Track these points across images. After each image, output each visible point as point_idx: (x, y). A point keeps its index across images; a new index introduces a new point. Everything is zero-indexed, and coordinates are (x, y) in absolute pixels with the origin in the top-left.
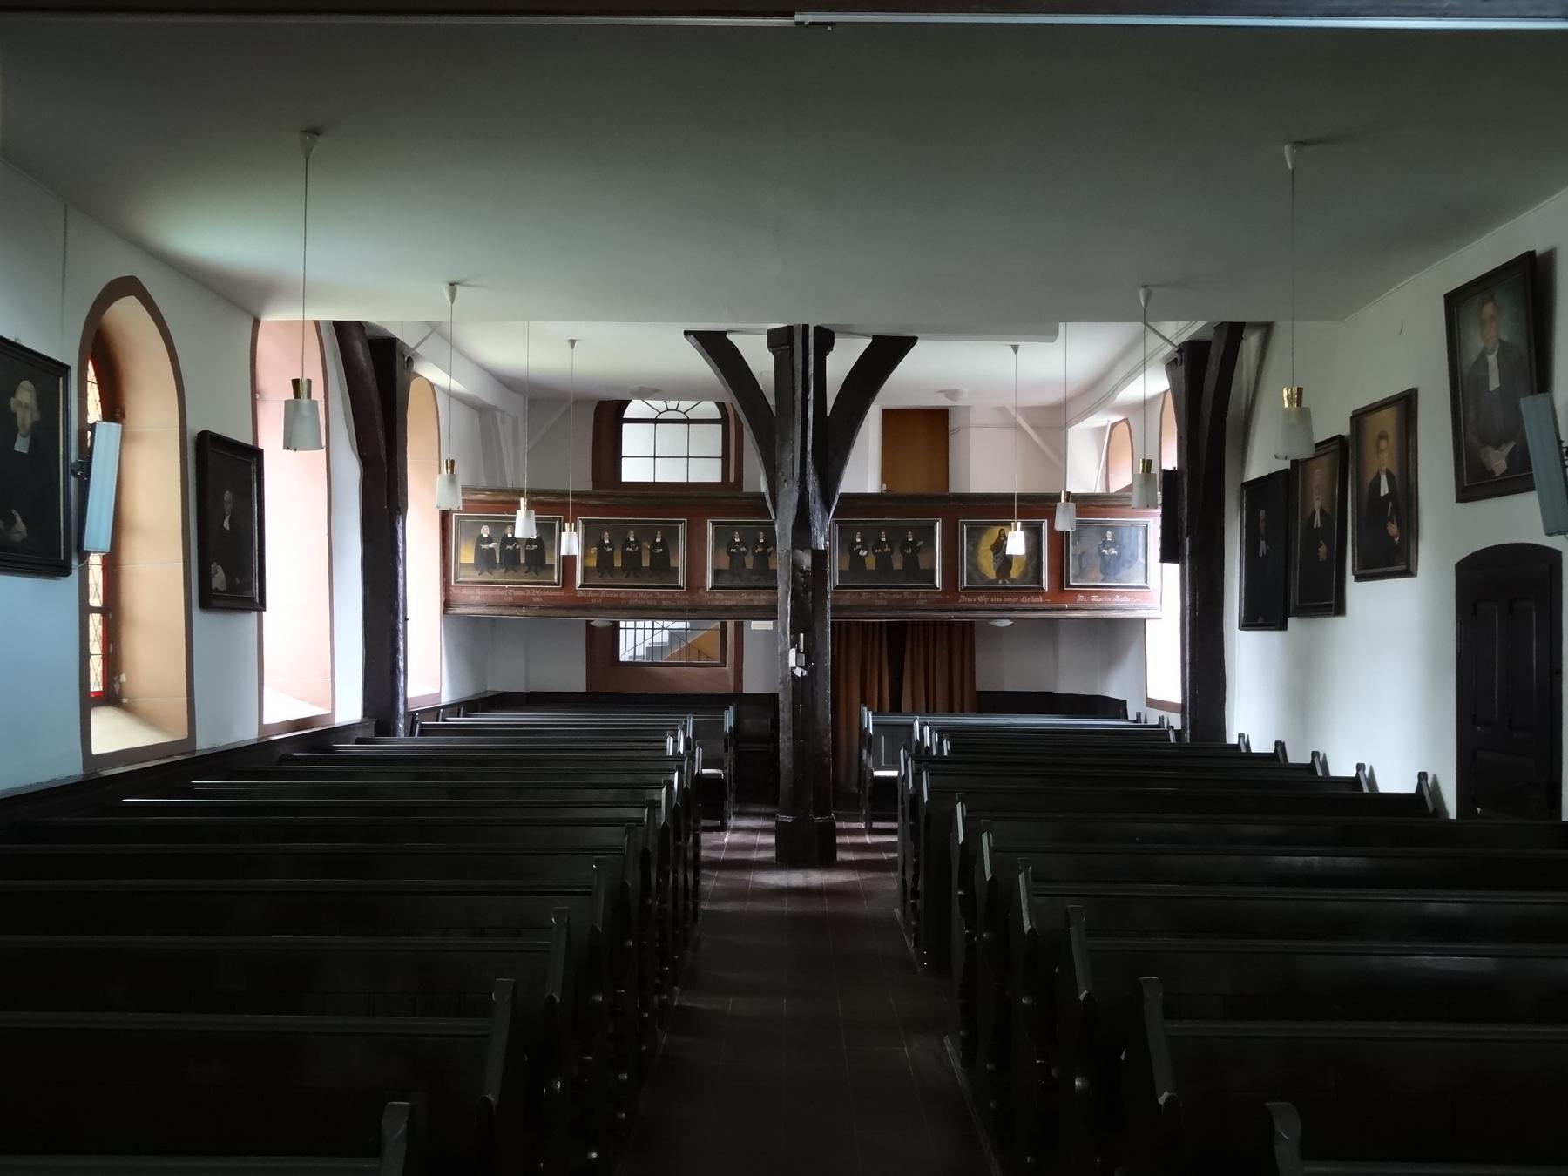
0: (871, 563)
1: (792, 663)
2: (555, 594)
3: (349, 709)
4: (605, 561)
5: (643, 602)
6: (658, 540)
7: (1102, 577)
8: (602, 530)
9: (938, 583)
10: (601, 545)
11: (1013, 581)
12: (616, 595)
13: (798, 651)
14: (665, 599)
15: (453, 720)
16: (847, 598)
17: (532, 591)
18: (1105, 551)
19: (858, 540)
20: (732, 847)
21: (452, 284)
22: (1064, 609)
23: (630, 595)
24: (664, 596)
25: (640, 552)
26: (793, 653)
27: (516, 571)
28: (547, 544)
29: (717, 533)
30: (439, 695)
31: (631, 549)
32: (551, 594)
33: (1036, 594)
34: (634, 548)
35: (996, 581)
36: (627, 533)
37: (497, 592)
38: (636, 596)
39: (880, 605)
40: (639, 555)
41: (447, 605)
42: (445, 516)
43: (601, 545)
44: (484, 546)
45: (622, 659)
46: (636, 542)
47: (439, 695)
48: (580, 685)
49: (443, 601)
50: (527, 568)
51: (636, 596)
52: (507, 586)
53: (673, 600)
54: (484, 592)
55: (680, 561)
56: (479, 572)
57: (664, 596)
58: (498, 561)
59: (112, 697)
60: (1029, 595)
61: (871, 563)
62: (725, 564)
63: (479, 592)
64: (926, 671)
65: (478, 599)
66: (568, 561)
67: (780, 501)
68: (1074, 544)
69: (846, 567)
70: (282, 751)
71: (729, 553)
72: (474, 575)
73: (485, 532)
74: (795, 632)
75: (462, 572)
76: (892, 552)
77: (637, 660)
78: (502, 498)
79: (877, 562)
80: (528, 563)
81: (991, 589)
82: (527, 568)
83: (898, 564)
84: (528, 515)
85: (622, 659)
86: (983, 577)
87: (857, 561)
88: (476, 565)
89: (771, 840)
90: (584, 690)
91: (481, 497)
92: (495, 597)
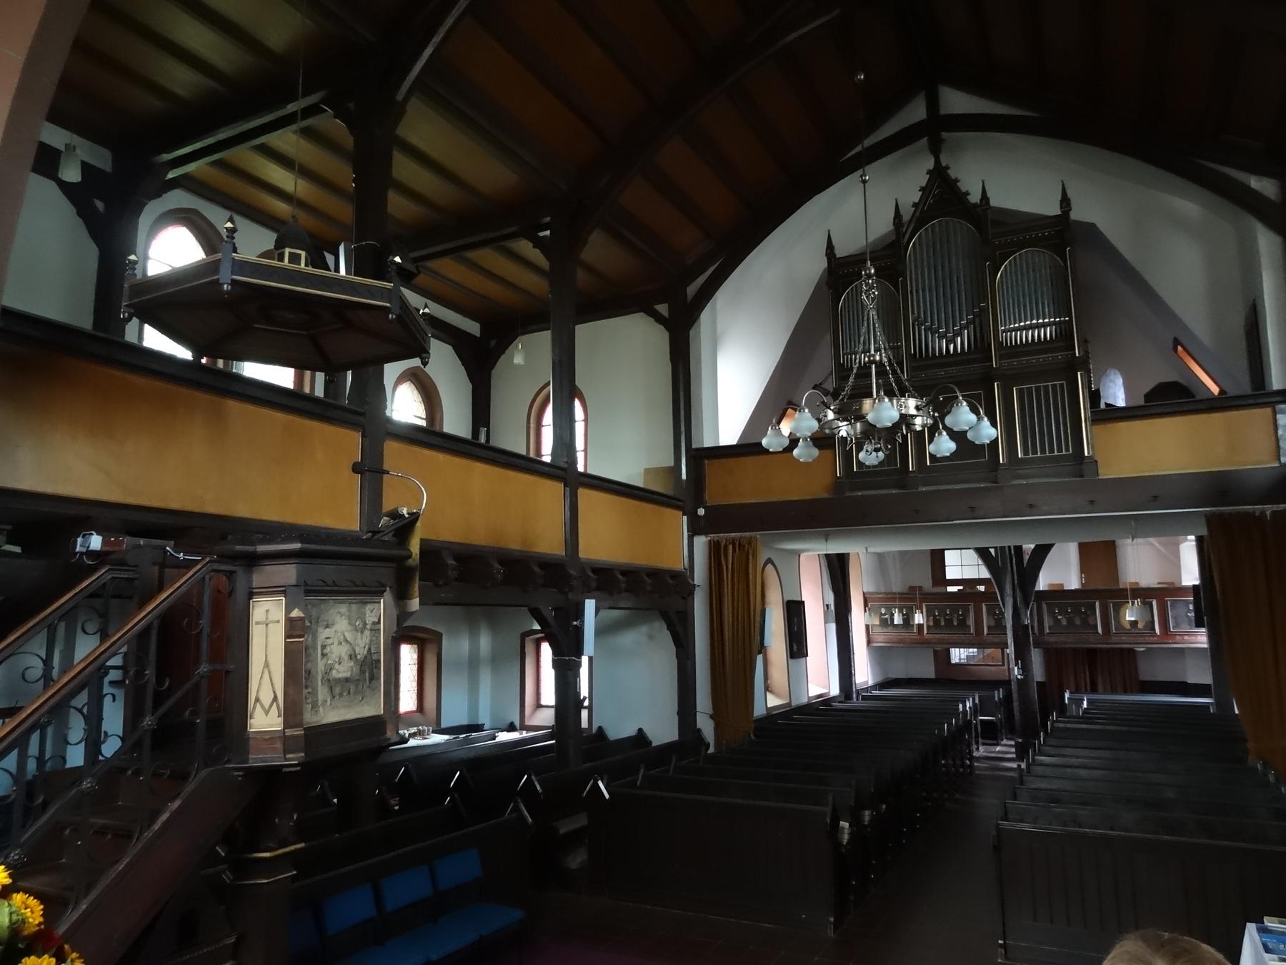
0: (1064, 622)
1: (1016, 673)
3: (835, 691)
4: (936, 622)
6: (960, 613)
7: (1188, 627)
9: (1100, 630)
10: (935, 616)
11: (1140, 630)
13: (1018, 668)
16: (1053, 639)
17: (906, 636)
18: (1189, 614)
19: (1057, 611)
20: (999, 752)
22: (1170, 643)
26: (1016, 668)
28: (911, 616)
29: (987, 609)
30: (867, 682)
32: (914, 637)
33: (1153, 636)
35: (1130, 630)
37: (890, 637)
39: (1068, 641)
40: (951, 620)
41: (869, 642)
42: (867, 627)
45: (953, 662)
47: (867, 682)
48: (932, 676)
54: (884, 637)
60: (1149, 636)
61: (1064, 622)
62: (993, 623)
63: (882, 637)
65: (881, 640)
66: (920, 626)
69: (1052, 624)
70: (816, 706)
71: (994, 619)
72: (880, 630)
73: (883, 611)
77: (962, 661)
78: (890, 596)
81: (1127, 633)
83: (1078, 622)
84: (899, 616)
85: (953, 662)
86: (1124, 628)
88: (880, 625)
89: (1013, 750)
91: (880, 596)
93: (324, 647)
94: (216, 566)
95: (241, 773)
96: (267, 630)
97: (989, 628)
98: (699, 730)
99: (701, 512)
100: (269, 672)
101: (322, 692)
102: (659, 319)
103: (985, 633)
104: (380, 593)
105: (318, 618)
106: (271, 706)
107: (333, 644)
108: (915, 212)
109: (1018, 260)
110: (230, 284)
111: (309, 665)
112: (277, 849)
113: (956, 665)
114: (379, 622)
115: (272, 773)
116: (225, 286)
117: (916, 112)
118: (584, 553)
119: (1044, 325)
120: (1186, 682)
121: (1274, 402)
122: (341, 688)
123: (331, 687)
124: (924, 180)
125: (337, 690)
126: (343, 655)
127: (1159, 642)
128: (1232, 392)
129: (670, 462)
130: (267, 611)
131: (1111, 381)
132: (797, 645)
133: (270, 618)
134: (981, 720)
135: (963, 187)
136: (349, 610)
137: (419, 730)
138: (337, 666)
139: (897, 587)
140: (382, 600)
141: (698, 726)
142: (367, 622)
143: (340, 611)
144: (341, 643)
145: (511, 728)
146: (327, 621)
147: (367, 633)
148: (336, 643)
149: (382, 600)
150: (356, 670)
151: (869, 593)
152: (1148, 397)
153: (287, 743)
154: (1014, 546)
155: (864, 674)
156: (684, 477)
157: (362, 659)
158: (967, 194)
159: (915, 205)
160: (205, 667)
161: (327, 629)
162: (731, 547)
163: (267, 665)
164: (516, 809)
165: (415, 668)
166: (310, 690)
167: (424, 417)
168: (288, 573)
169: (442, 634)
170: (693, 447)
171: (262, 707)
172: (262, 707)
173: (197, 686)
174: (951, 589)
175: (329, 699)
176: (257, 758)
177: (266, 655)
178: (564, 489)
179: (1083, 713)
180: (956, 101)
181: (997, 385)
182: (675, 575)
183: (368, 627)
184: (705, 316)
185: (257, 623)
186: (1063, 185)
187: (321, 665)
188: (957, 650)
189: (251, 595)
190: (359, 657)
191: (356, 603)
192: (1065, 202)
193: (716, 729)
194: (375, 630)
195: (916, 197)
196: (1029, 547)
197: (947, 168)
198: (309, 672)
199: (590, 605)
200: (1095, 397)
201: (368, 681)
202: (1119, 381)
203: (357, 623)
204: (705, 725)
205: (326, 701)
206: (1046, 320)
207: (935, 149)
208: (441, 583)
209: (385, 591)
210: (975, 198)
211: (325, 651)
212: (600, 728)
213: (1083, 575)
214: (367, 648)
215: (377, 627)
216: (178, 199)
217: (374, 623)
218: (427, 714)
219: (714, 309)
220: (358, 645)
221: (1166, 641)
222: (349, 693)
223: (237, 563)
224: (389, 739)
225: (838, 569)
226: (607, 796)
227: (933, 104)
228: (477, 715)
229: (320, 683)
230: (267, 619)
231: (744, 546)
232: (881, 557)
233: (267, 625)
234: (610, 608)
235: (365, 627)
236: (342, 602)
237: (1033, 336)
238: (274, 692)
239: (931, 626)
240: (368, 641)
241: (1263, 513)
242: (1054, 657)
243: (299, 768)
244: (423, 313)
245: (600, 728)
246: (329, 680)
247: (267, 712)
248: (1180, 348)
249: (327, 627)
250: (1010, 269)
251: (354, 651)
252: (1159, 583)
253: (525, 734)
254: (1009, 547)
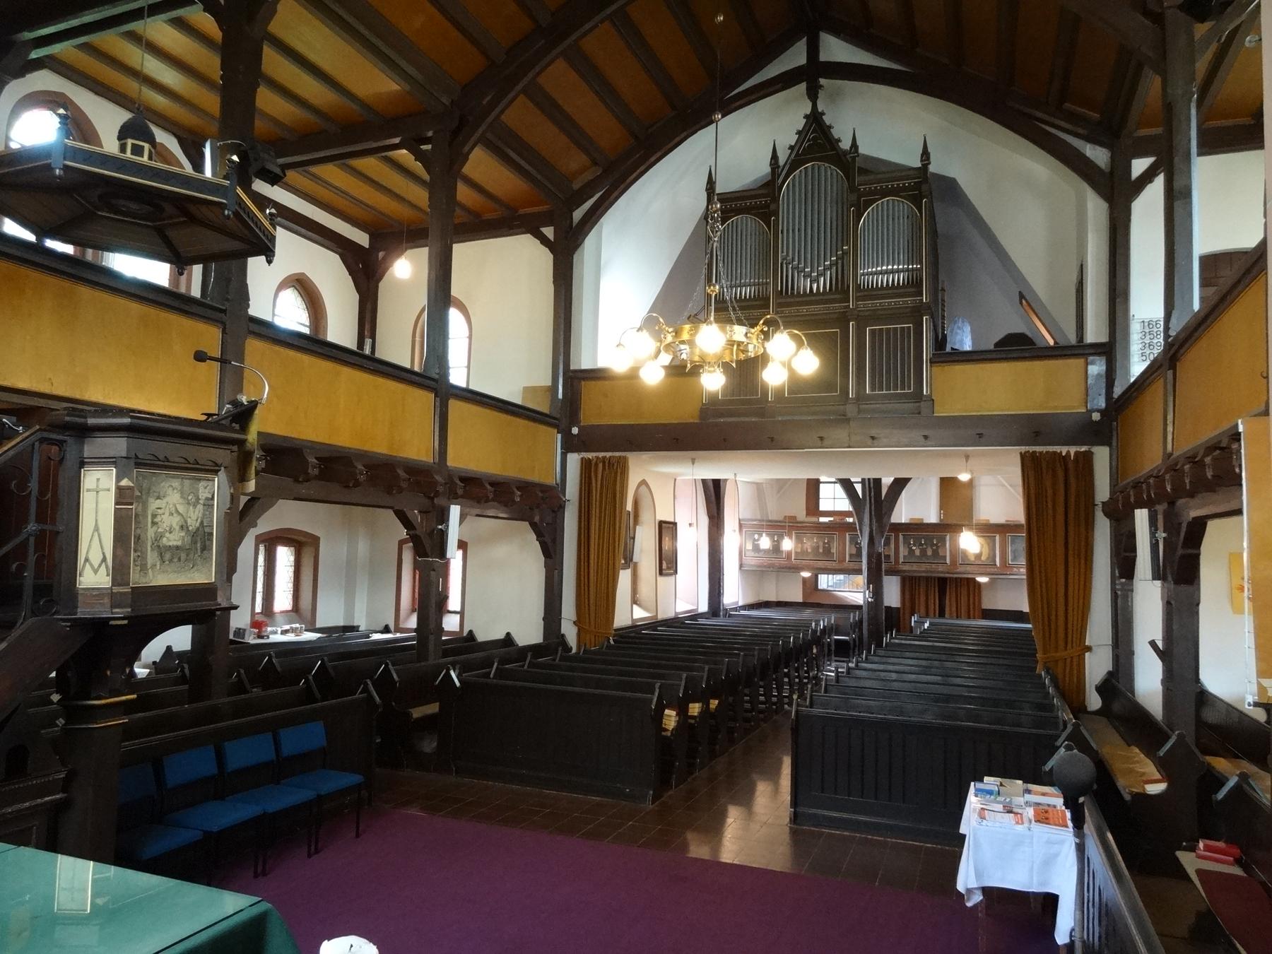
0: (918, 552)
2: (783, 562)
3: (704, 608)
13: (870, 591)
15: (743, 612)
16: (906, 567)
21: (735, 474)
22: (1007, 574)
26: (867, 592)
35: (974, 561)
37: (761, 561)
40: (818, 547)
41: (741, 566)
48: (800, 599)
55: (834, 550)
59: (635, 601)
61: (918, 552)
64: (957, 599)
67: (863, 531)
68: (1011, 546)
69: (906, 554)
72: (752, 554)
74: (869, 583)
79: (921, 552)
83: (929, 552)
86: (969, 560)
87: (911, 552)
90: (801, 601)
91: (755, 523)
93: (154, 516)
94: (46, 435)
95: (69, 624)
96: (97, 497)
97: (851, 555)
98: (563, 636)
99: (575, 430)
100: (99, 535)
101: (152, 557)
102: (544, 240)
103: (847, 560)
104: (216, 472)
105: (149, 489)
106: (100, 566)
107: (164, 514)
108: (791, 153)
109: (880, 208)
110: (62, 169)
111: (139, 531)
112: (108, 698)
113: (823, 590)
114: (213, 498)
115: (99, 625)
116: (58, 171)
117: (796, 56)
118: (451, 462)
119: (898, 271)
120: (1022, 611)
121: (1087, 354)
122: (170, 555)
123: (161, 554)
124: (800, 123)
125: (168, 556)
126: (174, 525)
127: (1001, 573)
128: (1062, 343)
129: (549, 383)
130: (98, 480)
131: (959, 328)
132: (667, 564)
133: (100, 487)
134: (836, 640)
135: (836, 133)
136: (182, 485)
137: (291, 628)
138: (167, 535)
139: (774, 516)
140: (216, 479)
141: (563, 632)
142: (200, 497)
143: (173, 485)
144: (172, 514)
145: (386, 630)
146: (159, 493)
147: (200, 507)
148: (167, 514)
149: (216, 479)
150: (188, 539)
151: (743, 520)
152: (997, 345)
153: (115, 600)
154: (873, 479)
155: (734, 594)
156: (560, 396)
157: (194, 531)
158: (839, 140)
159: (792, 148)
160: (34, 526)
161: (159, 500)
162: (601, 465)
163: (97, 529)
164: (366, 690)
165: (292, 569)
166: (139, 554)
167: (308, 324)
168: (118, 445)
169: (319, 538)
170: (571, 368)
171: (92, 566)
172: (92, 566)
173: (24, 544)
174: (822, 519)
175: (158, 563)
176: (83, 612)
177: (96, 520)
178: (435, 399)
179: (921, 633)
180: (836, 50)
181: (853, 324)
182: (545, 488)
183: (201, 502)
184: (589, 242)
185: (88, 490)
186: (925, 138)
187: (151, 533)
188: (826, 576)
189: (82, 464)
190: (190, 528)
191: (189, 479)
192: (925, 155)
193: (579, 635)
194: (209, 505)
195: (793, 139)
196: (887, 481)
197: (823, 114)
198: (138, 538)
199: (455, 511)
200: (940, 342)
201: (199, 551)
202: (968, 329)
203: (190, 498)
204: (569, 631)
205: (156, 565)
206: (901, 267)
207: (813, 94)
208: (300, 480)
209: (220, 470)
210: (845, 145)
211: (155, 520)
212: (471, 632)
213: (942, 512)
214: (199, 521)
215: (210, 502)
216: (44, 80)
217: (207, 499)
218: (300, 612)
219: (600, 234)
220: (190, 517)
221: (1005, 573)
222: (179, 560)
223: (67, 433)
224: (220, 604)
225: (714, 493)
226: (458, 684)
227: (813, 50)
228: (353, 618)
229: (149, 548)
230: (97, 486)
231: (613, 464)
232: (758, 487)
233: (97, 492)
234: (478, 515)
235: (198, 502)
236: (174, 477)
237: (893, 281)
238: (103, 554)
239: (798, 553)
240: (200, 515)
241: (1068, 452)
242: (910, 584)
243: (125, 622)
244: (270, 213)
245: (471, 632)
246: (159, 546)
247: (96, 571)
248: (1024, 301)
249: (158, 498)
250: (873, 215)
251: (187, 523)
252: (1007, 521)
253: (398, 635)
254: (869, 479)
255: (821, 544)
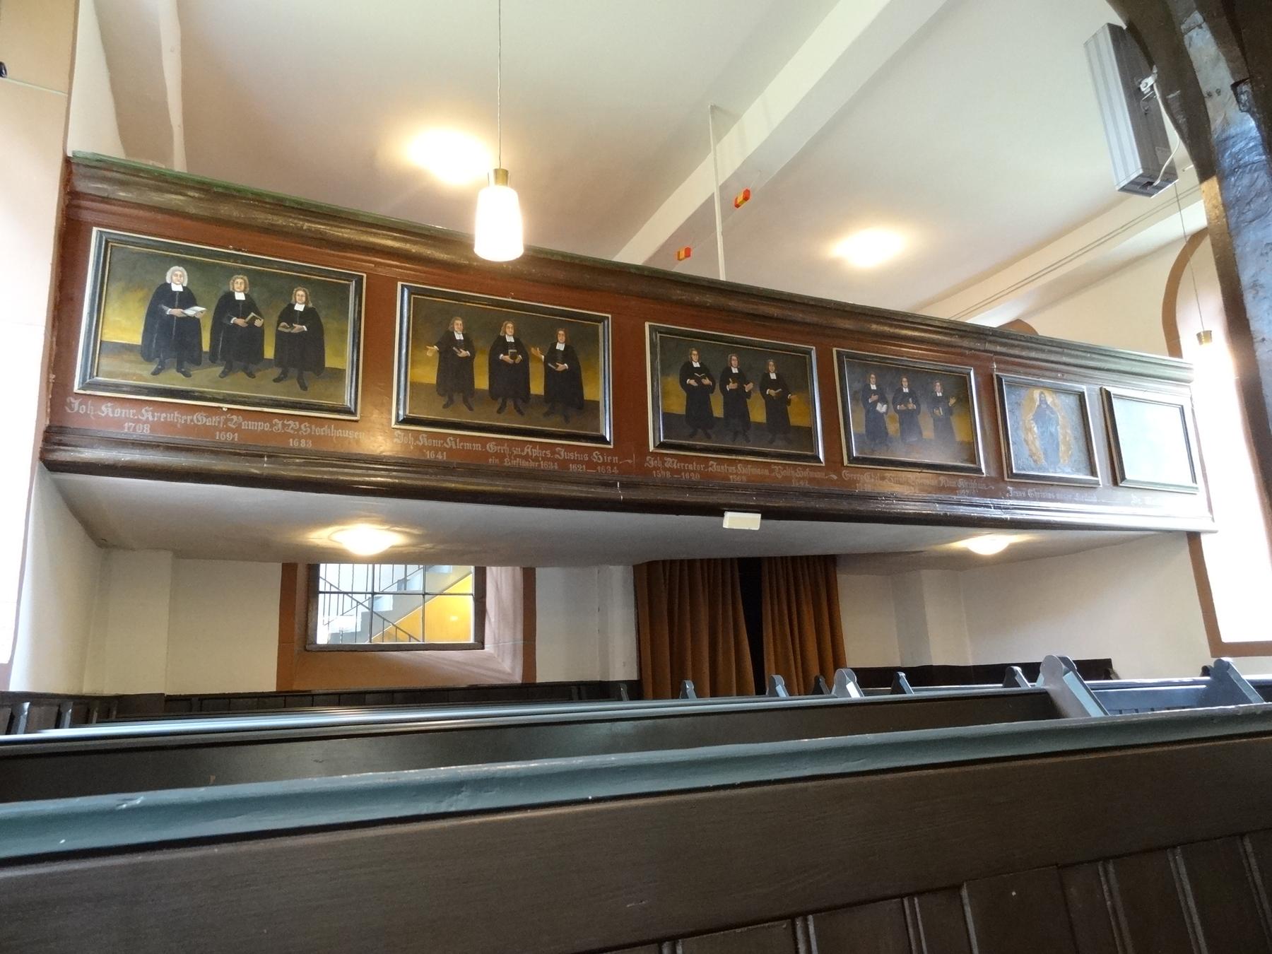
5: (532, 464)
8: (449, 315)
10: (447, 344)
12: (477, 447)
14: (574, 462)
19: (874, 387)
23: (505, 448)
24: (572, 456)
25: (525, 363)
27: (251, 375)
31: (507, 358)
34: (513, 356)
36: (499, 326)
37: (200, 419)
38: (517, 451)
40: (520, 374)
43: (447, 344)
44: (169, 311)
46: (517, 344)
49: (43, 428)
50: (277, 372)
51: (517, 451)
52: (225, 406)
53: (590, 464)
55: (599, 390)
56: (153, 367)
57: (572, 456)
58: (206, 346)
62: (678, 405)
63: (147, 414)
65: (144, 432)
72: (142, 373)
73: (177, 279)
75: (107, 363)
76: (918, 411)
80: (279, 360)
82: (277, 372)
88: (146, 352)
92: (188, 428)
97: (670, 421)
120: (932, 666)
151: (99, 166)
255: (538, 353)
